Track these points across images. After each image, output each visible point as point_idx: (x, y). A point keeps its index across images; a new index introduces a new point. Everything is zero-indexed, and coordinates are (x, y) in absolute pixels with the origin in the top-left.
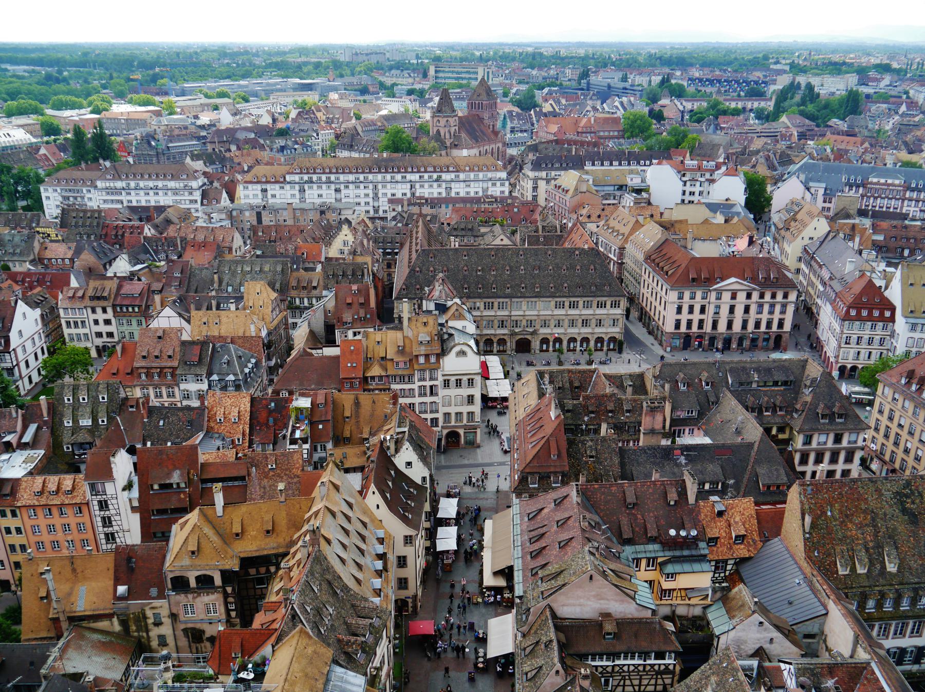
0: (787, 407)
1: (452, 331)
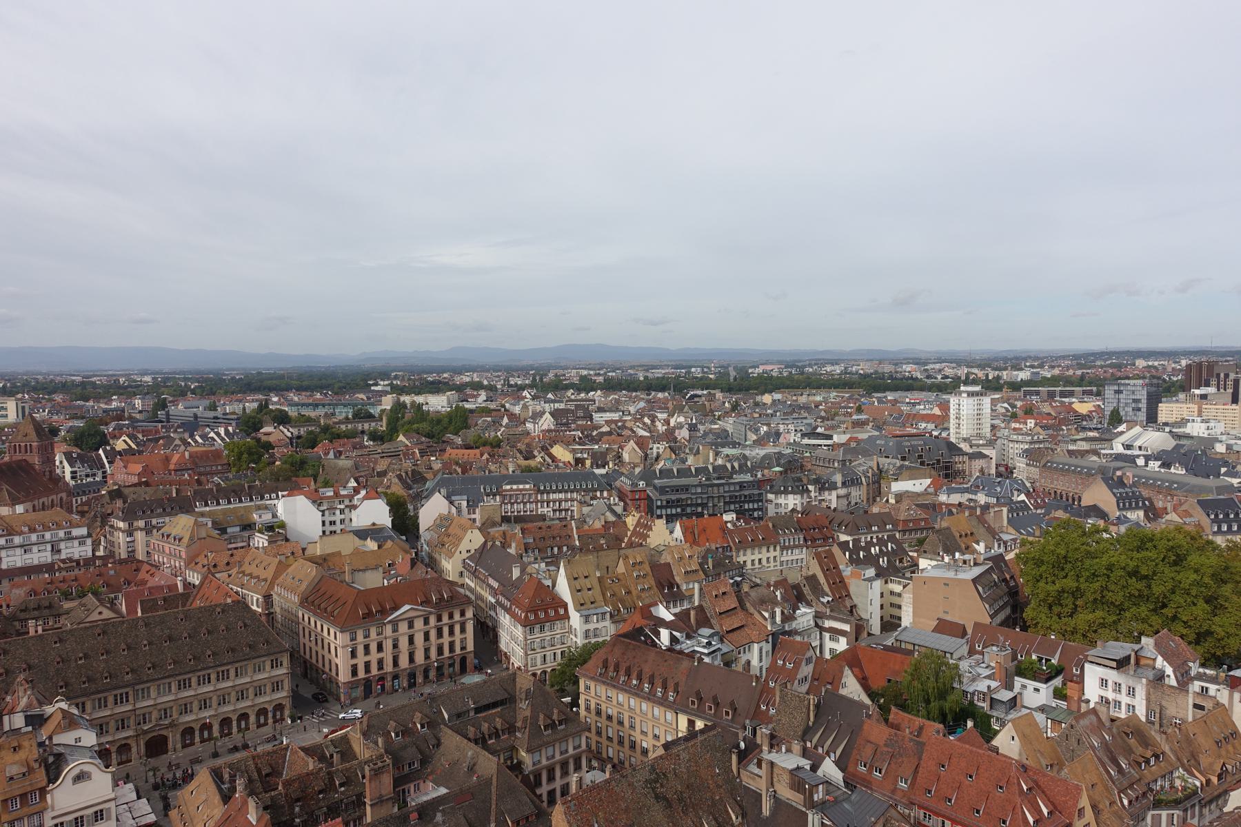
0: (509, 729)
1: (61, 750)
